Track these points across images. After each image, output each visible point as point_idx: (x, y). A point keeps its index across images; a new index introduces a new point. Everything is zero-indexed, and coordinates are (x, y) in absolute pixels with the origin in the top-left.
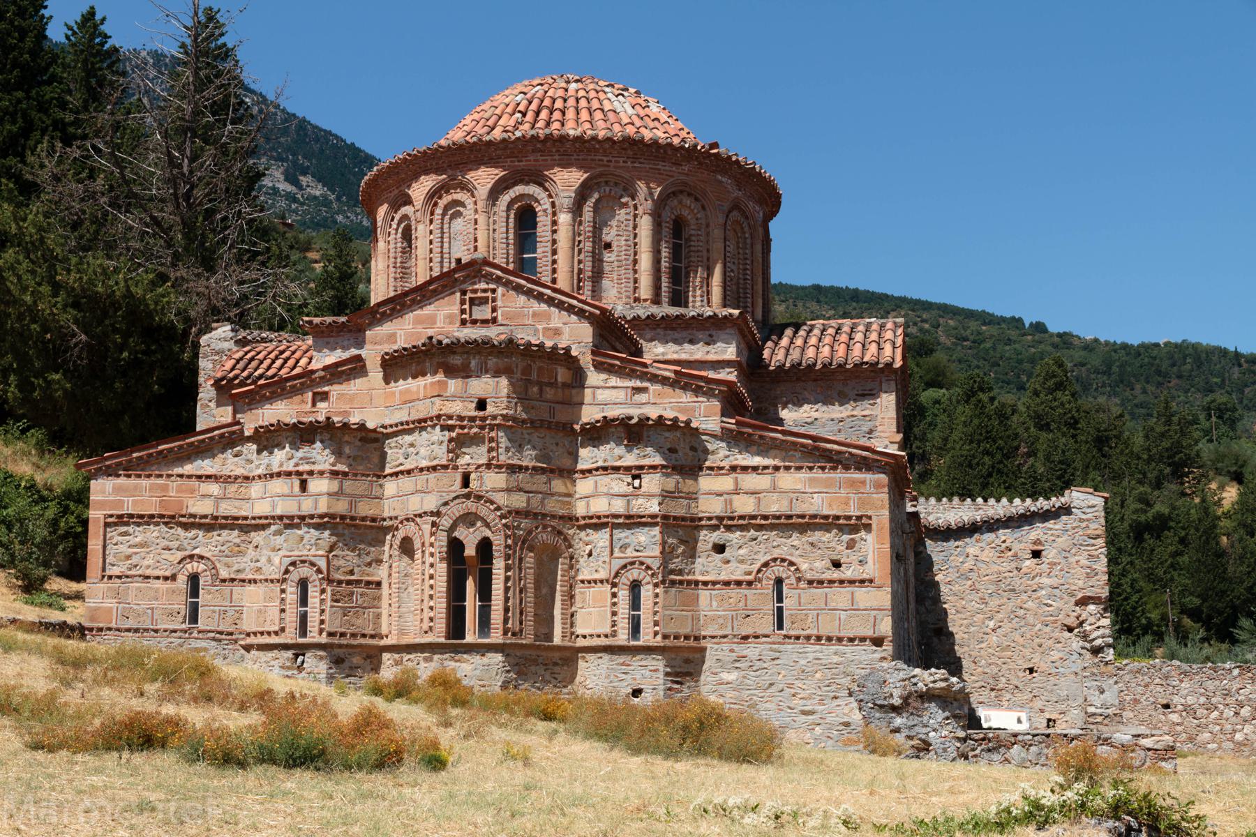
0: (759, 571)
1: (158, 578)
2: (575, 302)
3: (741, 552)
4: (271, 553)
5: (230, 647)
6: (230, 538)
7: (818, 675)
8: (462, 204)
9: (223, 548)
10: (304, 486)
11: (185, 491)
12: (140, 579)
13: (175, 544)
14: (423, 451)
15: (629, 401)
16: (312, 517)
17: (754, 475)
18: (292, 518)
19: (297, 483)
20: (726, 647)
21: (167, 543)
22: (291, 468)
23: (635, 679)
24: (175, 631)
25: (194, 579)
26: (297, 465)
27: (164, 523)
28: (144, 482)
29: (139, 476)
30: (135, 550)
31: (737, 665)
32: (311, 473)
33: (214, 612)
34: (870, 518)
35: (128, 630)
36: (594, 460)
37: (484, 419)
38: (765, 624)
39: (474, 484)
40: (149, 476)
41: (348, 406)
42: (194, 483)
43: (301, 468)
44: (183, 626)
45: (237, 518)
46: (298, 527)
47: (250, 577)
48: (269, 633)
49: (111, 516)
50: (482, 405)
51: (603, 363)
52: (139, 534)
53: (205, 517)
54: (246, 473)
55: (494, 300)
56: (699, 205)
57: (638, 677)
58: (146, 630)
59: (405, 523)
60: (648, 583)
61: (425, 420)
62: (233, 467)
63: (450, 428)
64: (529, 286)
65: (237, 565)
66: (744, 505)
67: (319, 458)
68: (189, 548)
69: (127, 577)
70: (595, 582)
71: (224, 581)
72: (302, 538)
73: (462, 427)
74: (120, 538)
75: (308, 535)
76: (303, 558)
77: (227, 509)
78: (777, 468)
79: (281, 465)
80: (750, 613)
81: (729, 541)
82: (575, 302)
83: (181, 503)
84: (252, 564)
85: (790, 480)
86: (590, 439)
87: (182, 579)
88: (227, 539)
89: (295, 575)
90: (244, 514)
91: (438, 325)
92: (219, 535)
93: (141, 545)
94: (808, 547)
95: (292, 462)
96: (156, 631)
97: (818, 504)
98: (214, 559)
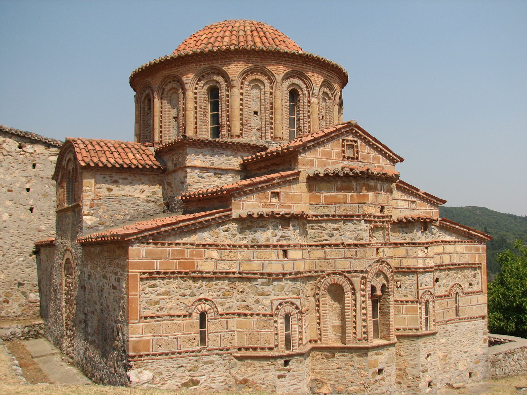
0: (451, 289)
1: (179, 316)
2: (391, 154)
3: (444, 281)
4: (258, 297)
5: (227, 358)
6: (223, 286)
7: (468, 335)
8: (262, 82)
9: (219, 293)
10: (285, 253)
11: (194, 255)
12: (168, 318)
13: (188, 292)
14: (348, 234)
15: (409, 208)
16: (290, 274)
17: (449, 245)
18: (277, 275)
19: (281, 252)
20: (442, 327)
21: (183, 291)
22: (275, 243)
23: (428, 349)
24: (192, 352)
25: (203, 316)
27: (180, 277)
29: (163, 244)
30: (161, 297)
31: (446, 334)
32: (289, 246)
33: (217, 336)
34: (481, 264)
35: (161, 354)
36: (403, 238)
37: (383, 217)
38: (452, 315)
39: (381, 254)
40: (170, 244)
41: (291, 202)
42: (201, 249)
43: (281, 243)
44: (198, 348)
45: (227, 273)
46: (280, 280)
47: (237, 311)
48: (263, 349)
49: (144, 273)
50: (382, 208)
51: (401, 187)
52: (163, 286)
53: (209, 272)
54: (233, 243)
55: (357, 147)
56: (168, 84)
57: (429, 348)
58: (173, 353)
59: (332, 275)
60: (431, 301)
61: (352, 216)
62: (224, 239)
63: (370, 222)
64: (373, 142)
65: (227, 304)
66: (447, 260)
67: (292, 236)
68: (197, 294)
69: (158, 317)
70: (407, 302)
71: (222, 315)
73: (376, 222)
74: (150, 289)
76: (287, 300)
77: (223, 267)
78: (455, 242)
79: (268, 240)
80: (448, 310)
81: (440, 276)
82: (391, 154)
83: (193, 263)
84: (239, 303)
85: (460, 248)
86: (400, 227)
87: (196, 317)
88: (221, 287)
89: (282, 312)
90: (233, 270)
91: (333, 158)
92: (216, 285)
93: (166, 293)
94: (463, 277)
95: (275, 239)
96: (180, 353)
97: (467, 259)
98: (214, 300)
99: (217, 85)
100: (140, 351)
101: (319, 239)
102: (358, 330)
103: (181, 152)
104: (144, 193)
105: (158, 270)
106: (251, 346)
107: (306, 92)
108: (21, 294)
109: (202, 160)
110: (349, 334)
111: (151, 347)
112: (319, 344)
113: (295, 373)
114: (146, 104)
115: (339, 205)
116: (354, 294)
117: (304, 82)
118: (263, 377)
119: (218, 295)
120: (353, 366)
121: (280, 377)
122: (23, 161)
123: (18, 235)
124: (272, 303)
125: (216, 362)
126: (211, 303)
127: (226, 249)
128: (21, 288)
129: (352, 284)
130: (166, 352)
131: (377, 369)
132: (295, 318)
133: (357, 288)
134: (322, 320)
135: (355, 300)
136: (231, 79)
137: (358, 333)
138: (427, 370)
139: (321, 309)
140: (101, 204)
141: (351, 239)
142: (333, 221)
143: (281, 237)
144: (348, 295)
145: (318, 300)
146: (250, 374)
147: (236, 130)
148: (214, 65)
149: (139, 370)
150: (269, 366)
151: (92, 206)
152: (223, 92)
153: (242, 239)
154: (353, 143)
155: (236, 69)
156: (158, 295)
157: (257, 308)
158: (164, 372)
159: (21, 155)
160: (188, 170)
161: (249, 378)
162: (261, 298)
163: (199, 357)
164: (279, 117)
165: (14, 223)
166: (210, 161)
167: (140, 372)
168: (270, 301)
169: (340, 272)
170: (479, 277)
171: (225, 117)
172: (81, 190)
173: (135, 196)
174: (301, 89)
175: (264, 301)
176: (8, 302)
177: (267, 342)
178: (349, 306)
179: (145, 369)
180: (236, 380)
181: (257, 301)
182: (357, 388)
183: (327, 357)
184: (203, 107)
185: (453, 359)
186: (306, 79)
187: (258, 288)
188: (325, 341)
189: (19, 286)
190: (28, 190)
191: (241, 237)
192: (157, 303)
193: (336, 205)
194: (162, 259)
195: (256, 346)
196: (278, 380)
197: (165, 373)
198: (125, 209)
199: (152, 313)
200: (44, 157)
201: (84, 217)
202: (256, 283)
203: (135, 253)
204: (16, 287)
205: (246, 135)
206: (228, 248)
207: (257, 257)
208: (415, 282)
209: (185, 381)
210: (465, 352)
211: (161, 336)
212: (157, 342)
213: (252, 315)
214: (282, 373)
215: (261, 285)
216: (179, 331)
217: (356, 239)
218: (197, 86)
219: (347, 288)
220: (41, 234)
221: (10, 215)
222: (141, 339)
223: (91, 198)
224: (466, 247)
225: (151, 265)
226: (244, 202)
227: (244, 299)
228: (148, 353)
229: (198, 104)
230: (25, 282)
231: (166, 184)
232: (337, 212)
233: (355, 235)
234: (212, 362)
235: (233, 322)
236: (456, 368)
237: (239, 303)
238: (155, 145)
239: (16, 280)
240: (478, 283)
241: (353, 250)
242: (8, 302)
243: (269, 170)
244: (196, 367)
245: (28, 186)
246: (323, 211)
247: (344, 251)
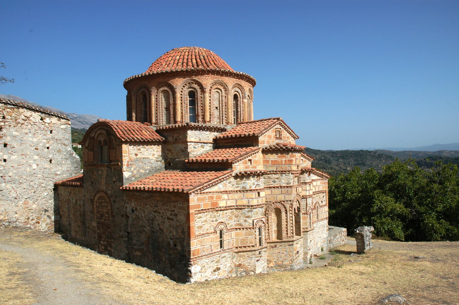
4: (246, 218)
9: (227, 218)
10: (259, 193)
13: (214, 219)
14: (283, 181)
16: (261, 205)
21: (213, 219)
22: (254, 188)
26: (255, 187)
28: (207, 196)
30: (203, 223)
32: (260, 190)
41: (256, 165)
45: (230, 206)
58: (209, 254)
59: (275, 203)
61: (285, 171)
62: (229, 188)
65: (230, 224)
72: (258, 212)
75: (259, 211)
83: (217, 203)
87: (219, 232)
89: (258, 226)
90: (233, 205)
91: (272, 139)
92: (226, 213)
93: (206, 221)
96: (212, 254)
98: (225, 222)
100: (195, 255)
101: (268, 184)
102: (288, 232)
103: (182, 132)
104: (155, 156)
105: (202, 209)
106: (243, 245)
107: (241, 96)
108: (47, 217)
109: (195, 137)
110: (284, 235)
111: (200, 252)
112: (268, 241)
113: (264, 258)
114: (141, 97)
115: (279, 166)
116: (286, 213)
117: (240, 90)
118: (249, 262)
119: (227, 220)
120: (286, 251)
121: (258, 261)
122: (44, 129)
123: (43, 178)
124: (253, 221)
125: (227, 257)
126: (224, 224)
127: (231, 193)
128: (47, 213)
129: (285, 208)
130: (206, 254)
131: (296, 251)
132: (263, 228)
133: (288, 210)
134: (270, 228)
135: (287, 216)
136: (204, 87)
137: (288, 234)
138: (310, 249)
139: (269, 222)
140: (133, 164)
141: (284, 183)
142: (275, 174)
143: (257, 185)
144: (283, 214)
145: (268, 218)
146: (242, 261)
147: (207, 119)
148: (194, 78)
149: (195, 266)
150: (252, 255)
151: (128, 165)
152: (199, 94)
153: (237, 187)
154: (279, 130)
155: (207, 81)
156: (202, 222)
157: (246, 225)
158: (205, 266)
159: (42, 124)
160: (189, 144)
161: (242, 263)
162: (247, 219)
163: (220, 255)
164: (230, 111)
165: (40, 170)
166: (199, 138)
167: (196, 267)
168: (252, 221)
169: (279, 201)
170: (325, 197)
171: (200, 110)
172: (121, 156)
173: (150, 158)
174: (239, 94)
175: (249, 220)
176: (39, 223)
177: (251, 243)
178: (284, 219)
179: (198, 265)
180: (235, 265)
181: (245, 221)
182: (288, 262)
183: (272, 247)
184: (186, 103)
185: (316, 241)
186: (242, 88)
187: (245, 214)
188: (271, 239)
189: (45, 212)
190: (48, 148)
191: (236, 186)
192: (201, 227)
193: (277, 166)
194: (204, 202)
195: (245, 245)
196: (256, 263)
197: (206, 266)
198: (146, 166)
199: (200, 233)
200: (57, 126)
201: (124, 173)
202: (245, 211)
203: (192, 200)
204: (44, 213)
205: (212, 121)
206: (231, 192)
207: (245, 197)
208: (305, 203)
209: (214, 269)
210: (320, 237)
211: (204, 245)
212: (203, 249)
213: (243, 229)
214: (258, 259)
215: (247, 212)
216: (212, 242)
217: (287, 184)
218: (182, 90)
219: (283, 210)
220: (58, 177)
221: (37, 165)
222: (196, 248)
223: (127, 160)
224: (321, 182)
225: (199, 206)
226: (237, 166)
227: (238, 220)
228: (199, 256)
229: (183, 101)
230: (49, 209)
231: (166, 150)
232: (278, 169)
233: (287, 182)
234: (225, 257)
235: (233, 233)
236: (317, 246)
237: (235, 223)
238: (153, 124)
239: (43, 208)
240: (324, 201)
241: (286, 189)
242: (39, 223)
243: (235, 144)
244: (219, 261)
245: (48, 146)
246: (270, 169)
247: (282, 190)
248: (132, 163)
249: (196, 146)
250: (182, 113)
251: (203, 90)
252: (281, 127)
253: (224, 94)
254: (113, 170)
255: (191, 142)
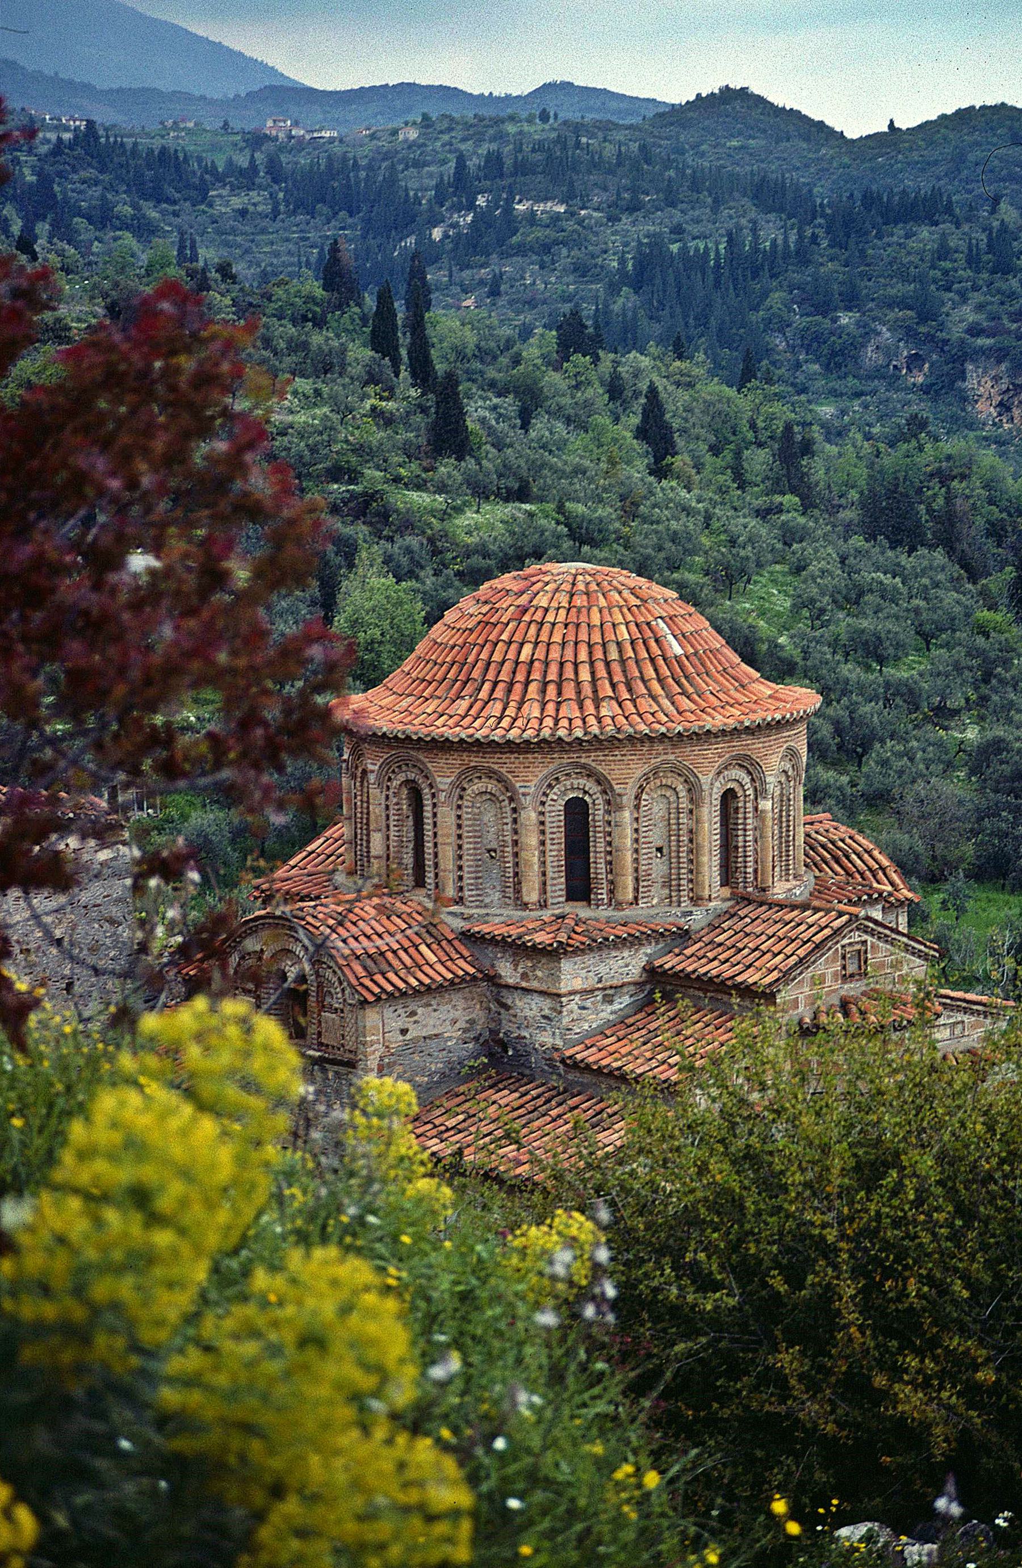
99: (587, 798)
104: (458, 1025)
140: (395, 1063)
152: (598, 813)
171: (603, 866)
218: (544, 799)
223: (378, 1054)
248: (393, 1059)
249: (588, 1004)
250: (544, 874)
251: (613, 805)
252: (865, 937)
253: (684, 804)
254: (330, 1075)
255: (571, 993)
